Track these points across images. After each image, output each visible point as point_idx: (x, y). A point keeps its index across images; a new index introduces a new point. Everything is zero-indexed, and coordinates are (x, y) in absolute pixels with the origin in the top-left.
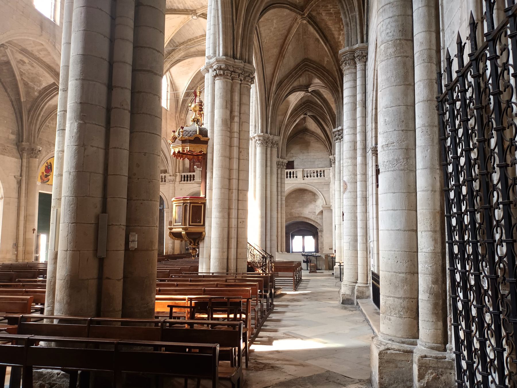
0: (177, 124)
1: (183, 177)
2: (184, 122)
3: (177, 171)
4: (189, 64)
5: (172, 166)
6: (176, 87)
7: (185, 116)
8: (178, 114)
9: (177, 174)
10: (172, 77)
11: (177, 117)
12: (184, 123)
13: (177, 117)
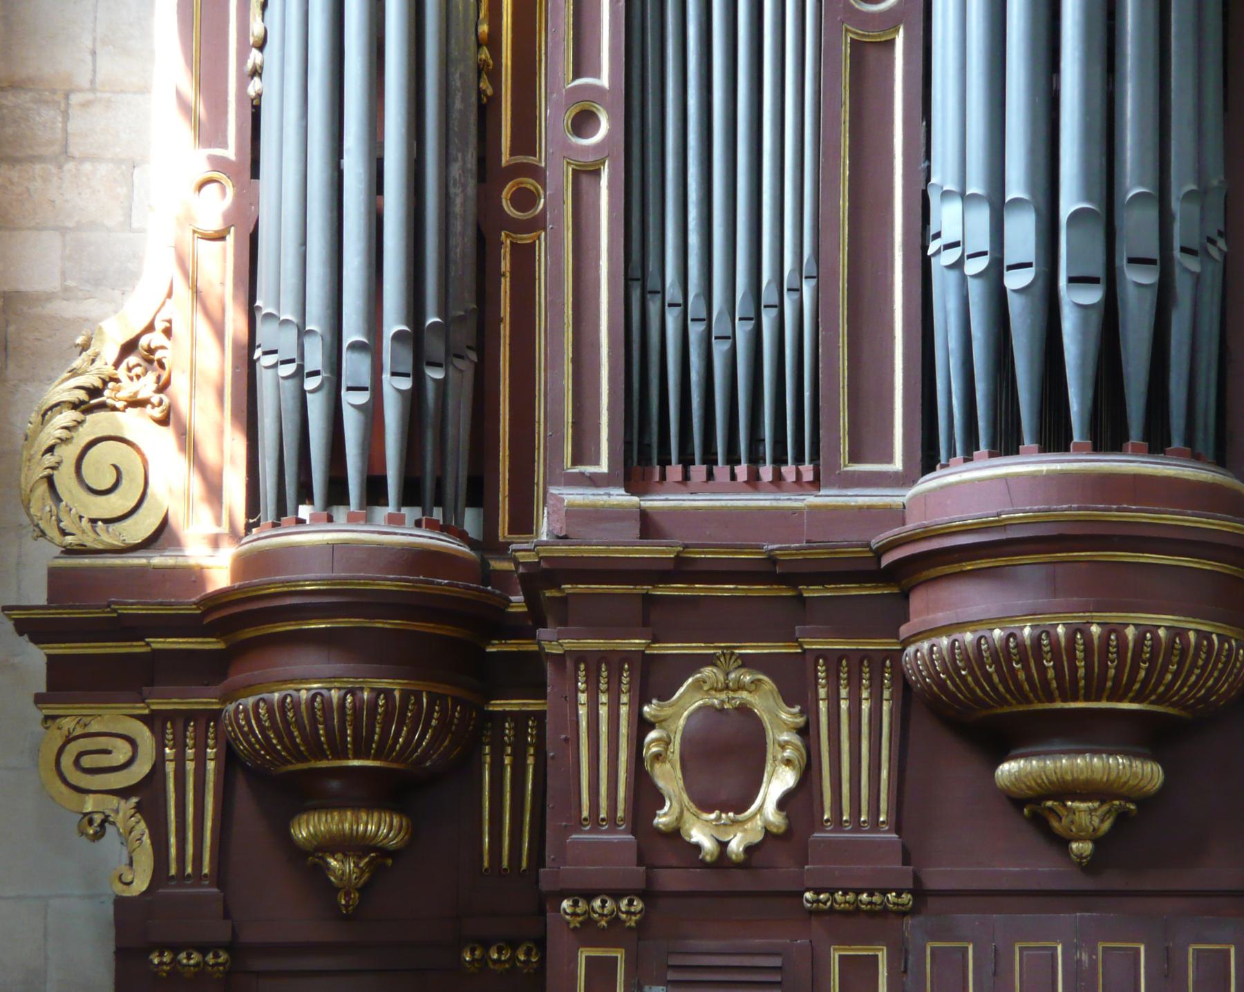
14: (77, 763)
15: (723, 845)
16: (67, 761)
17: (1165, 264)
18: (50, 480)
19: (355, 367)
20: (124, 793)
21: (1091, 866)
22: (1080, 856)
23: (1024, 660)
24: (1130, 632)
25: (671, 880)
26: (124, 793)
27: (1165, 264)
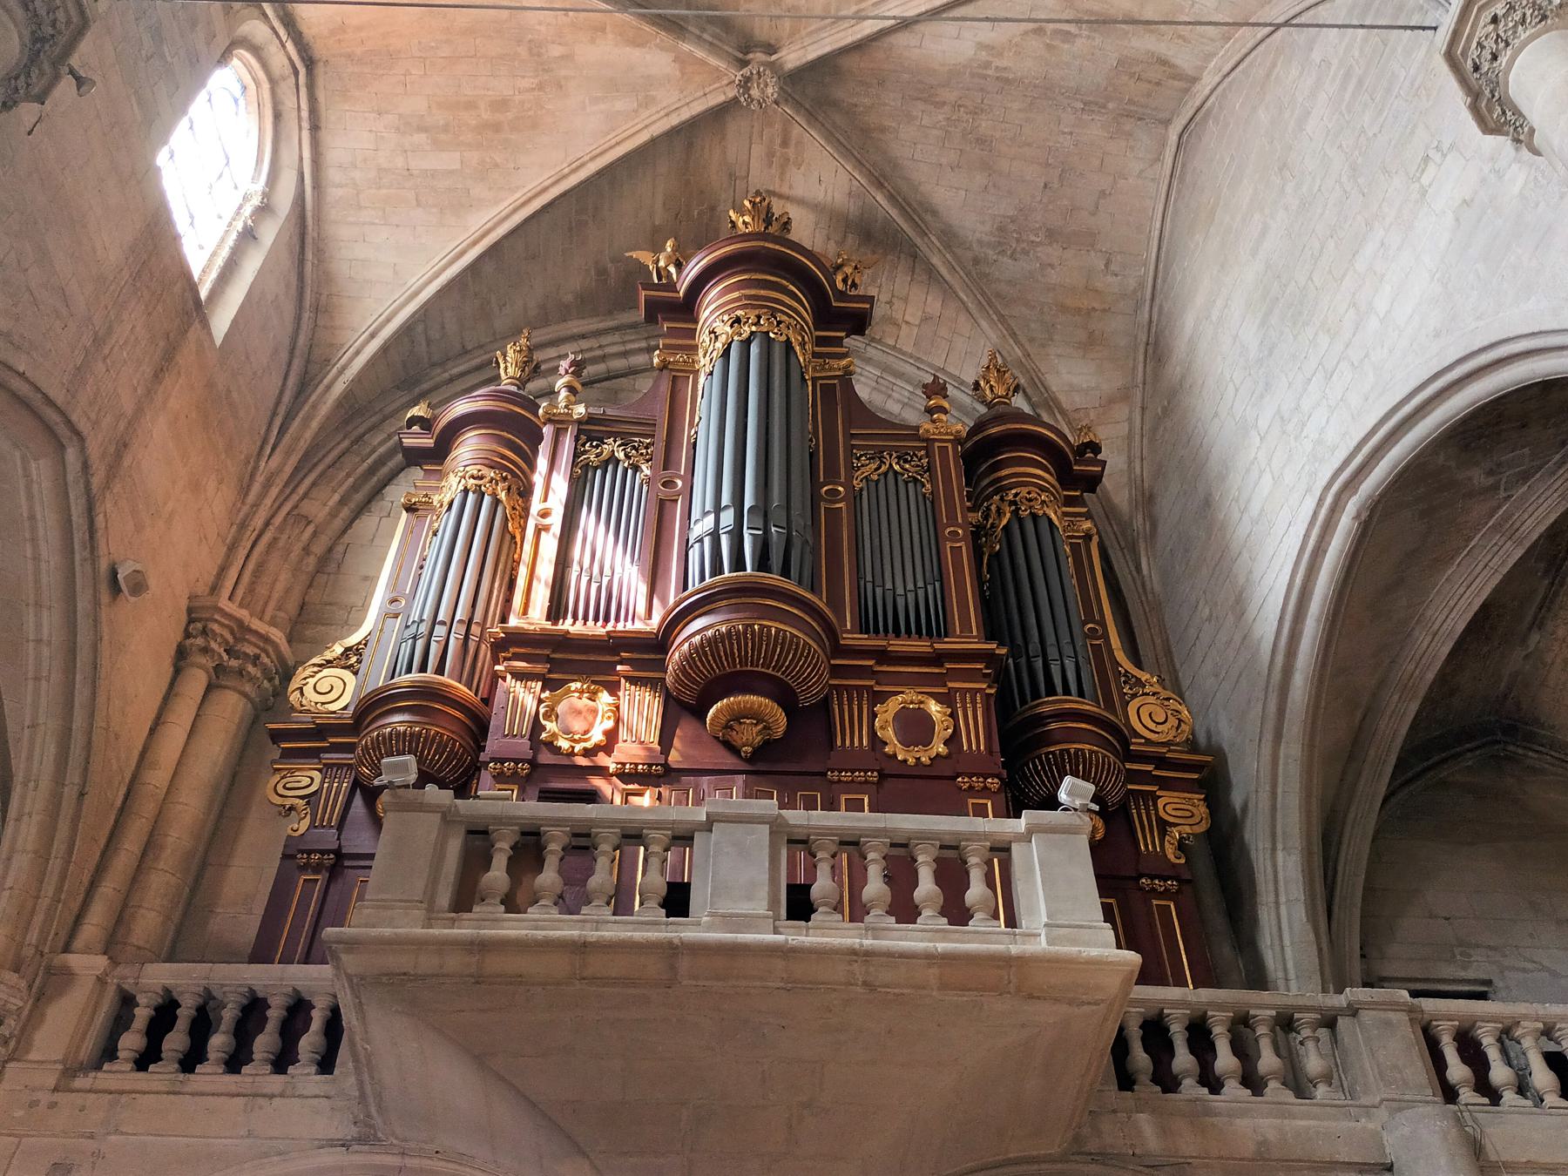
0: (243, 526)
1: (142, 1014)
2: (319, 548)
3: (92, 929)
4: (497, 128)
5: (43, 855)
6: (326, 278)
7: (345, 512)
8: (280, 463)
9: (74, 960)
10: (317, 185)
11: (260, 479)
12: (311, 562)
13: (260, 479)
14: (284, 787)
15: (573, 748)
16: (280, 788)
17: (789, 528)
18: (301, 689)
19: (440, 631)
20: (302, 797)
21: (750, 760)
22: (746, 752)
23: (723, 642)
24: (773, 630)
25: (545, 758)
26: (302, 797)
27: (789, 528)
